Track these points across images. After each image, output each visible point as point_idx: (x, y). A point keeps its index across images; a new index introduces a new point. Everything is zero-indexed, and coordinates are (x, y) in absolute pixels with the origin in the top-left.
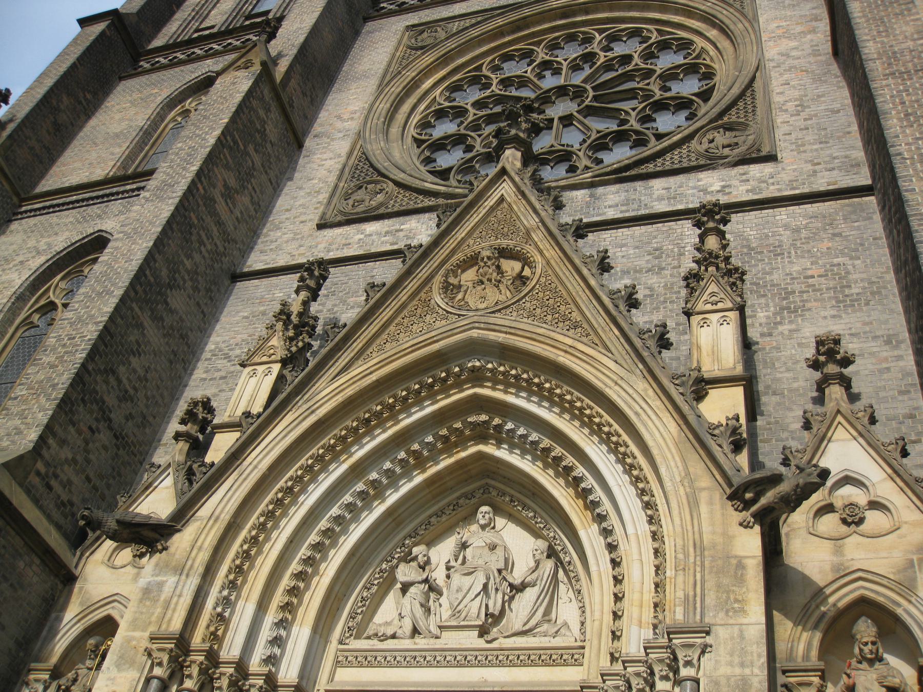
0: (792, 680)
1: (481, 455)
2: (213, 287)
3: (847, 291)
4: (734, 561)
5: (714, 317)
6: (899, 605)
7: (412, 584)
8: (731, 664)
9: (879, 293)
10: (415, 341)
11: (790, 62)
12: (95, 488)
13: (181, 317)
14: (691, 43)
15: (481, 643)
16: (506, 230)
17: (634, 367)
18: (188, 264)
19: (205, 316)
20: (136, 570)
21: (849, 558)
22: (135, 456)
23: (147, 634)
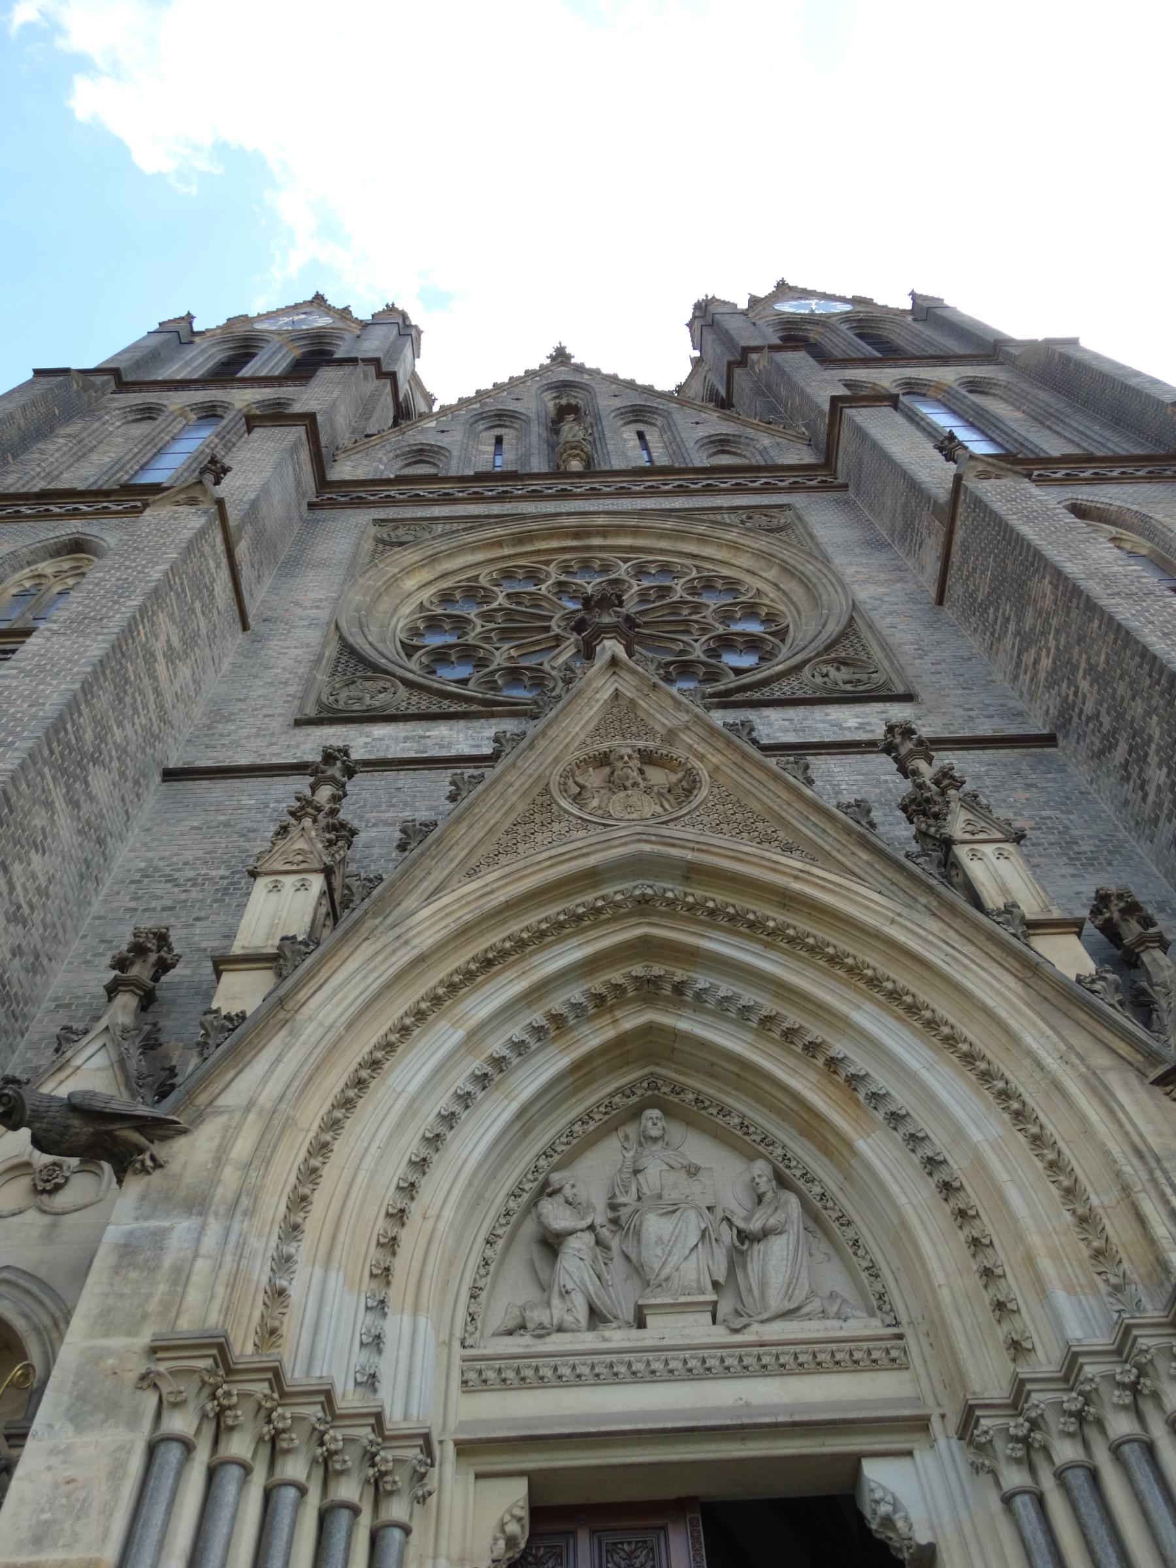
1: (650, 1029)
2: (142, 780)
3: (1076, 848)
5: (988, 849)
7: (571, 1233)
9: (1119, 852)
10: (553, 852)
11: (885, 607)
13: (101, 810)
14: (739, 582)
15: (719, 1335)
16: (634, 729)
17: (911, 902)
19: (128, 819)
20: (47, 1219)
22: (16, 1020)
23: (144, 1339)
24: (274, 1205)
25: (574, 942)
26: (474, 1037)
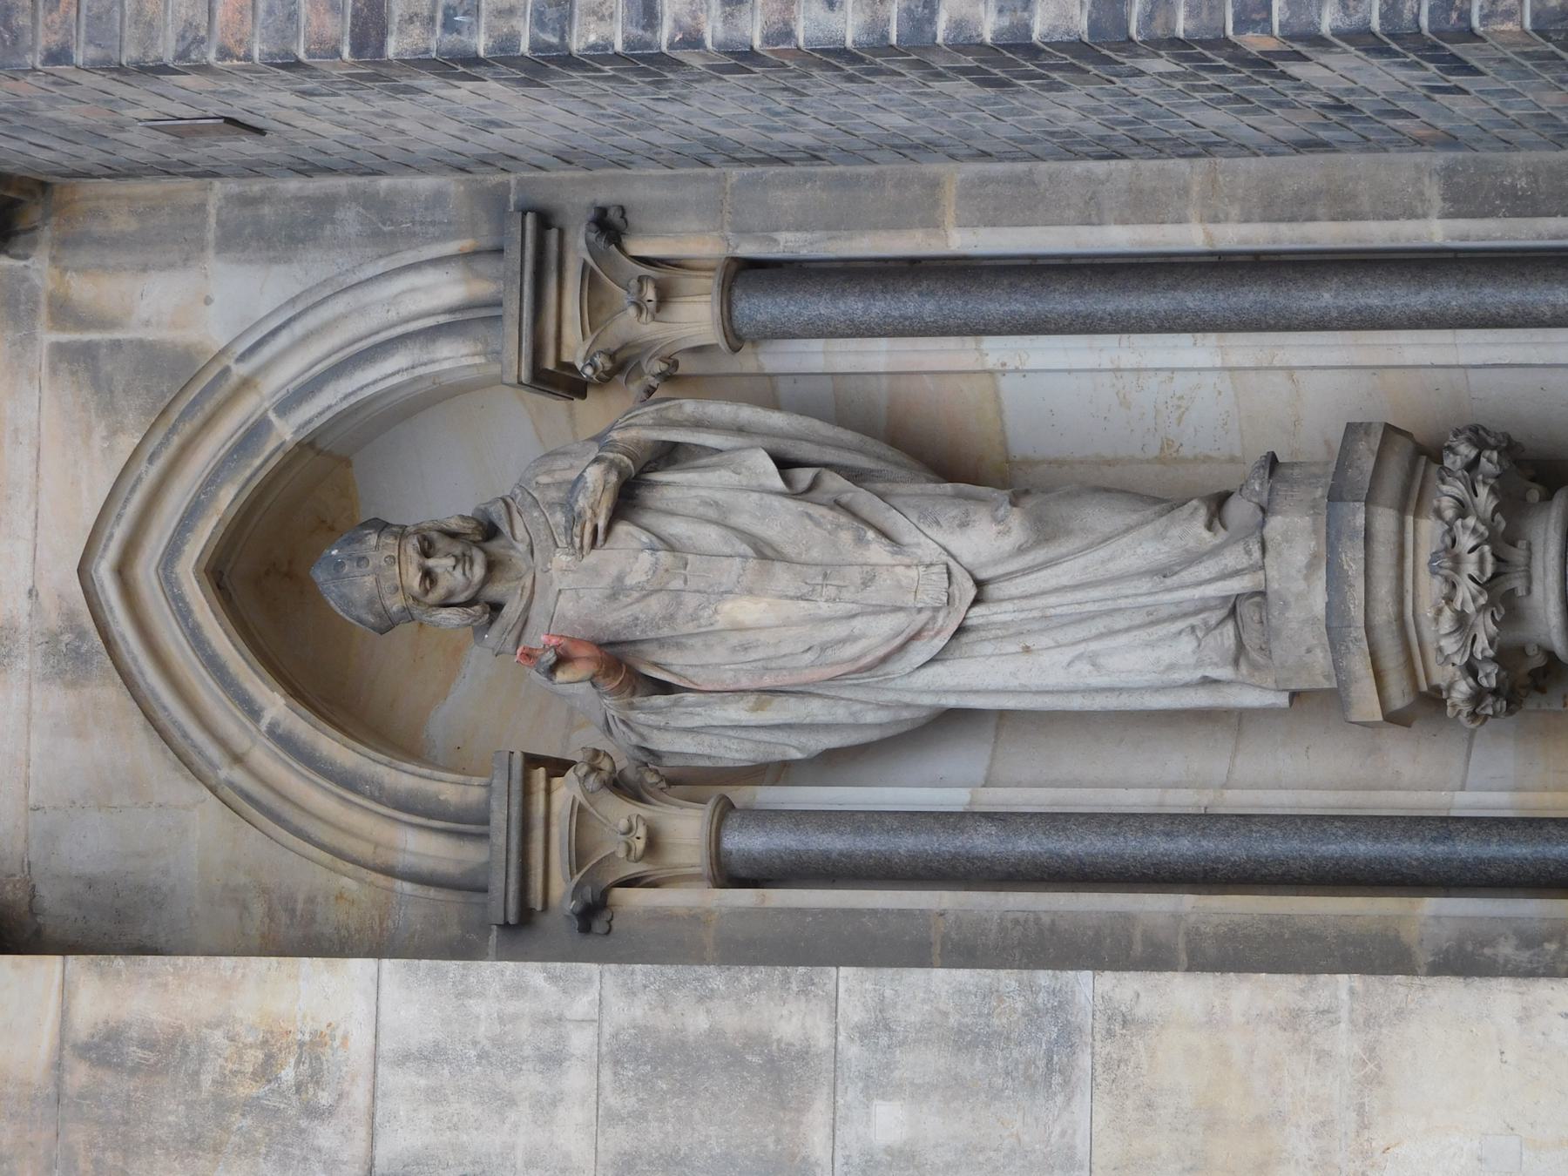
0: (561, 886)
4: (79, 1075)
6: (256, 431)
8: (546, 1106)
21: (24, 605)
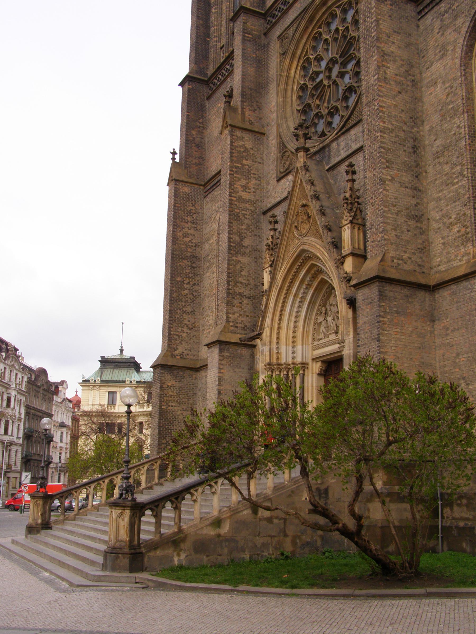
12: (251, 317)
18: (244, 227)
24: (275, 340)
25: (303, 269)
26: (295, 296)
